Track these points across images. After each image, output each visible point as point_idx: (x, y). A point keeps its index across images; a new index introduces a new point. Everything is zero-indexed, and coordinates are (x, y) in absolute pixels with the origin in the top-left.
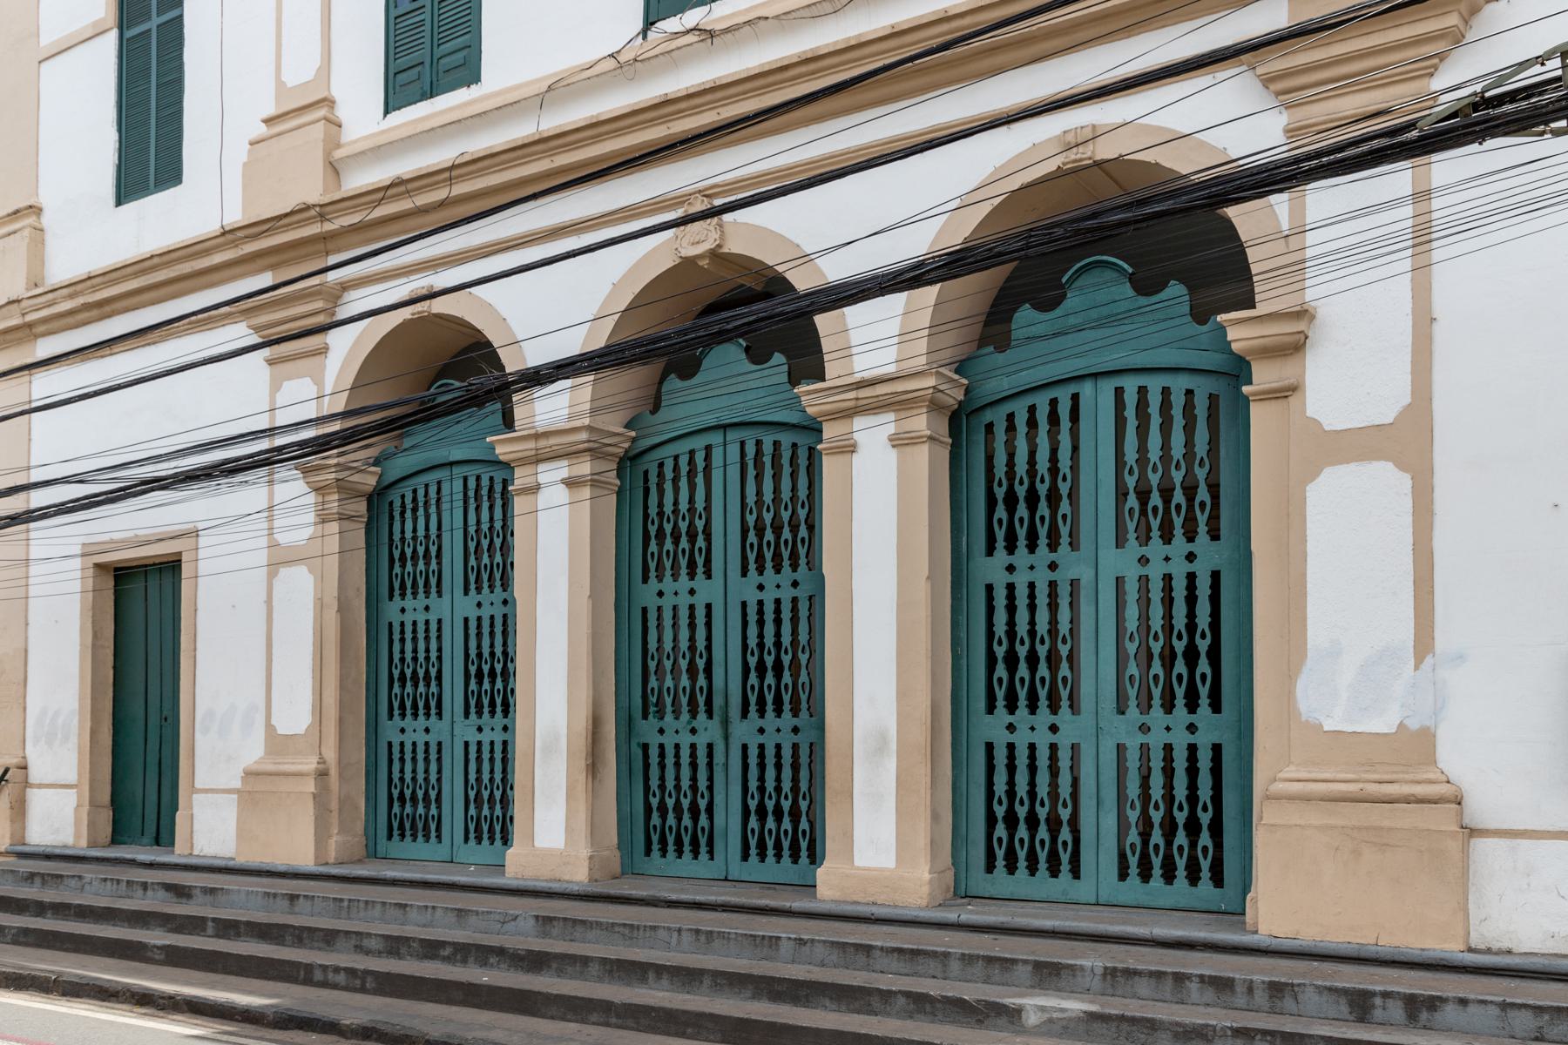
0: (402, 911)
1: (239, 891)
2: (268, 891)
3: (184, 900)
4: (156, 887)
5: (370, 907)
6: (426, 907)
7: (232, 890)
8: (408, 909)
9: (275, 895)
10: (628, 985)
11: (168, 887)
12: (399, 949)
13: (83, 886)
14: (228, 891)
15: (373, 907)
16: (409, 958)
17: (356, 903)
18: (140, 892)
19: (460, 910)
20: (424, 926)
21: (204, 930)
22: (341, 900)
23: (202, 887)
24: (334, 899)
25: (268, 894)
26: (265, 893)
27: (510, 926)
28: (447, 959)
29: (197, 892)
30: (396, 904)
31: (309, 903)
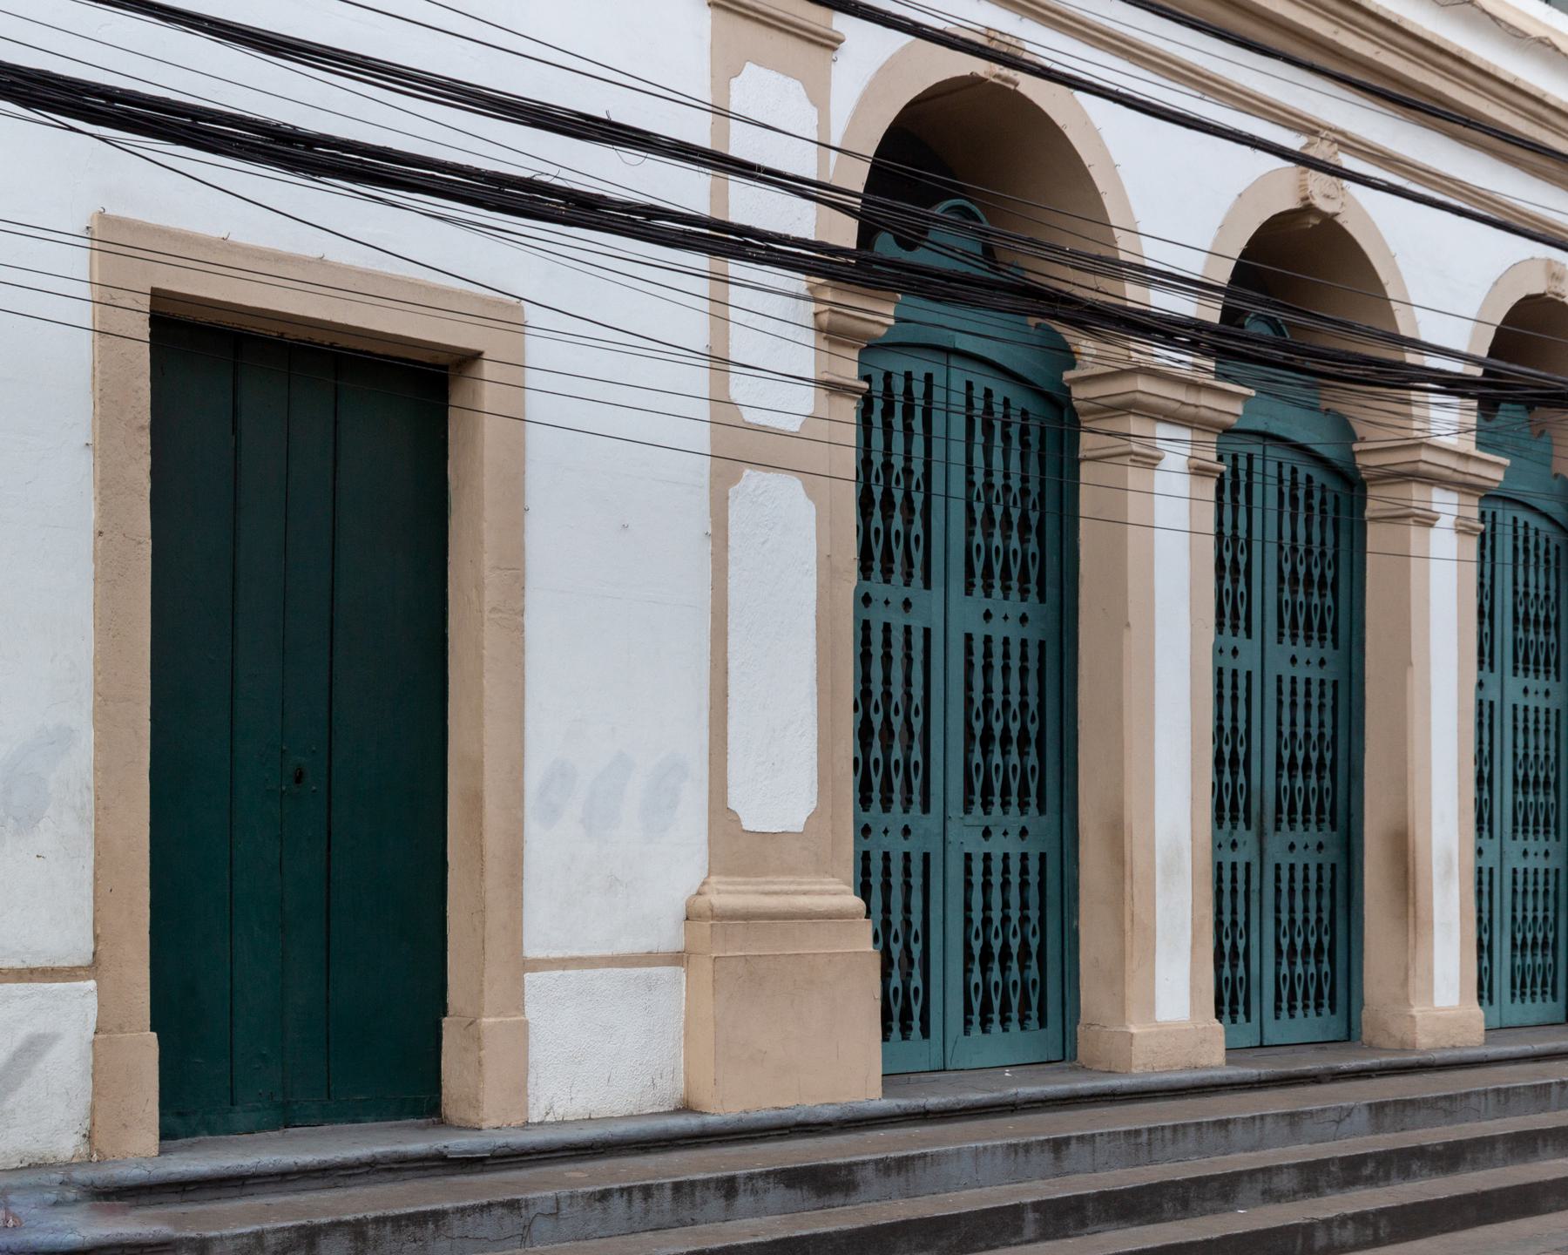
0: (1223, 1133)
1: (959, 1152)
2: (1014, 1141)
3: (838, 1198)
4: (760, 1184)
5: (1180, 1135)
6: (1253, 1118)
7: (946, 1154)
8: (1231, 1127)
9: (1027, 1147)
10: (1525, 1161)
11: (792, 1178)
12: (1317, 1180)
13: (527, 1227)
14: (935, 1159)
15: (1185, 1134)
16: (1328, 1191)
17: (1159, 1135)
18: (716, 1204)
19: (1292, 1115)
20: (1252, 1149)
21: (1018, 1231)
22: (1137, 1133)
23: (877, 1162)
24: (1125, 1132)
25: (1014, 1148)
26: (1010, 1146)
27: (1345, 1126)
28: (1371, 1181)
29: (869, 1173)
30: (1215, 1123)
31: (1088, 1148)
